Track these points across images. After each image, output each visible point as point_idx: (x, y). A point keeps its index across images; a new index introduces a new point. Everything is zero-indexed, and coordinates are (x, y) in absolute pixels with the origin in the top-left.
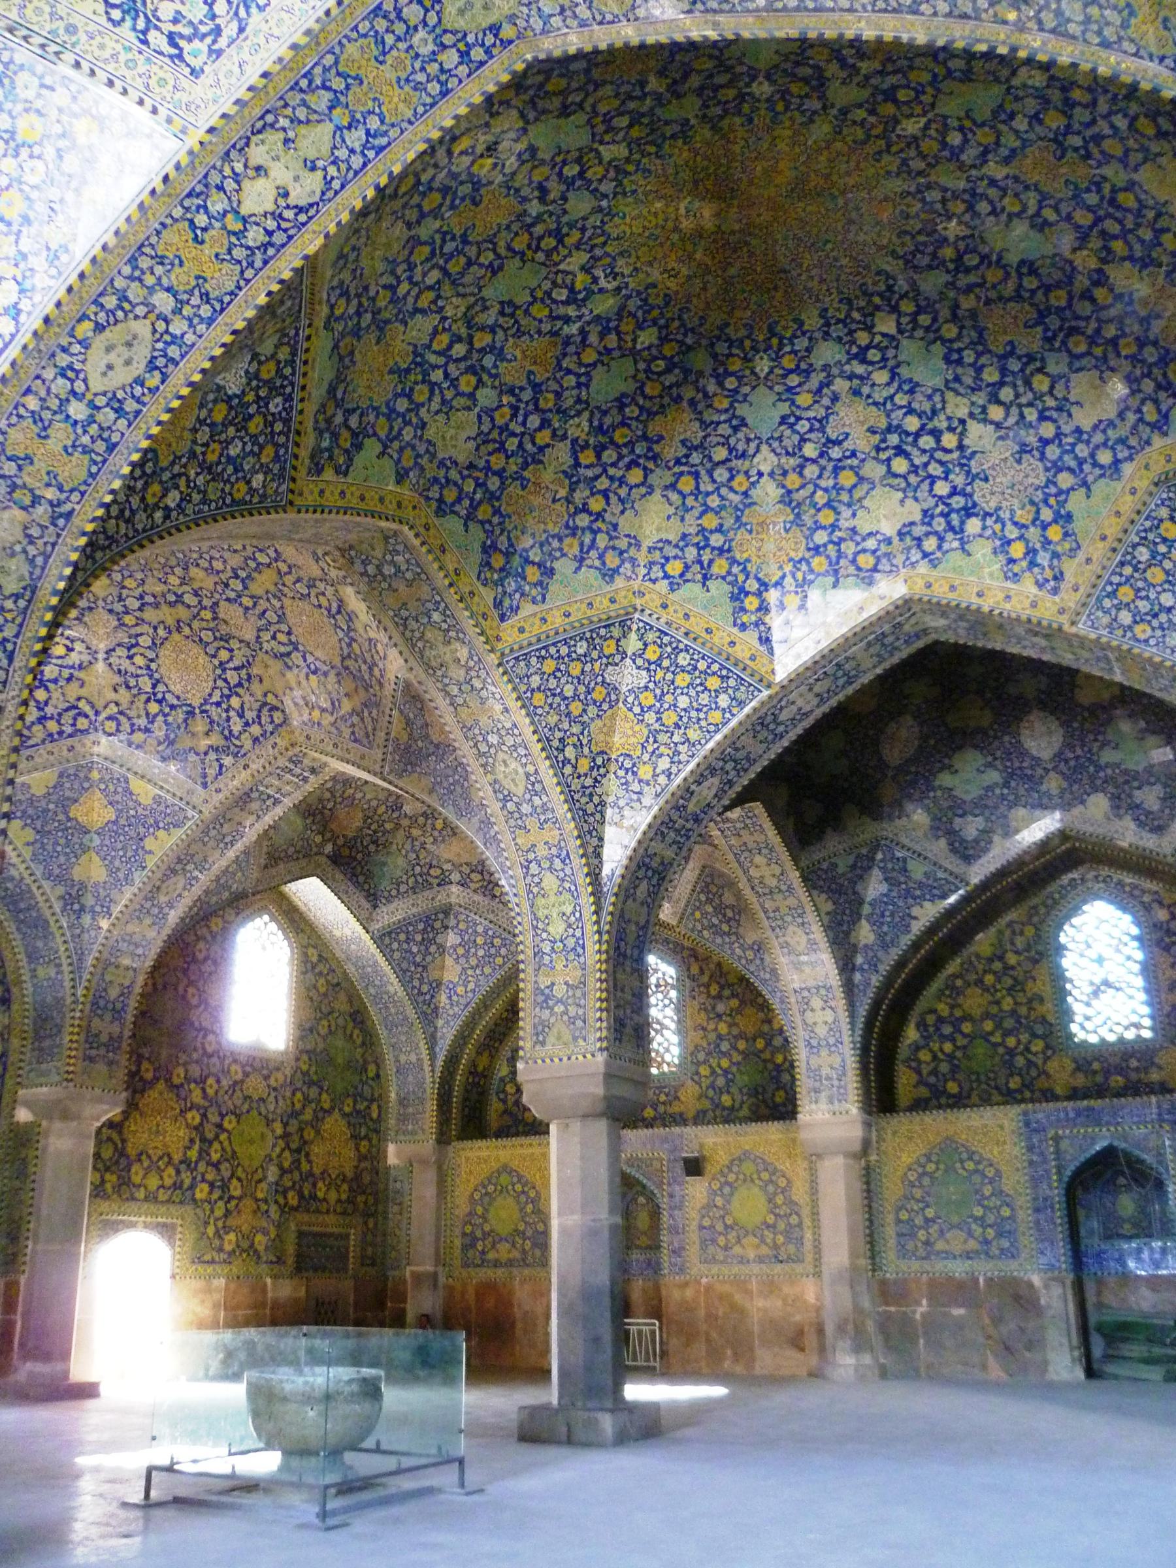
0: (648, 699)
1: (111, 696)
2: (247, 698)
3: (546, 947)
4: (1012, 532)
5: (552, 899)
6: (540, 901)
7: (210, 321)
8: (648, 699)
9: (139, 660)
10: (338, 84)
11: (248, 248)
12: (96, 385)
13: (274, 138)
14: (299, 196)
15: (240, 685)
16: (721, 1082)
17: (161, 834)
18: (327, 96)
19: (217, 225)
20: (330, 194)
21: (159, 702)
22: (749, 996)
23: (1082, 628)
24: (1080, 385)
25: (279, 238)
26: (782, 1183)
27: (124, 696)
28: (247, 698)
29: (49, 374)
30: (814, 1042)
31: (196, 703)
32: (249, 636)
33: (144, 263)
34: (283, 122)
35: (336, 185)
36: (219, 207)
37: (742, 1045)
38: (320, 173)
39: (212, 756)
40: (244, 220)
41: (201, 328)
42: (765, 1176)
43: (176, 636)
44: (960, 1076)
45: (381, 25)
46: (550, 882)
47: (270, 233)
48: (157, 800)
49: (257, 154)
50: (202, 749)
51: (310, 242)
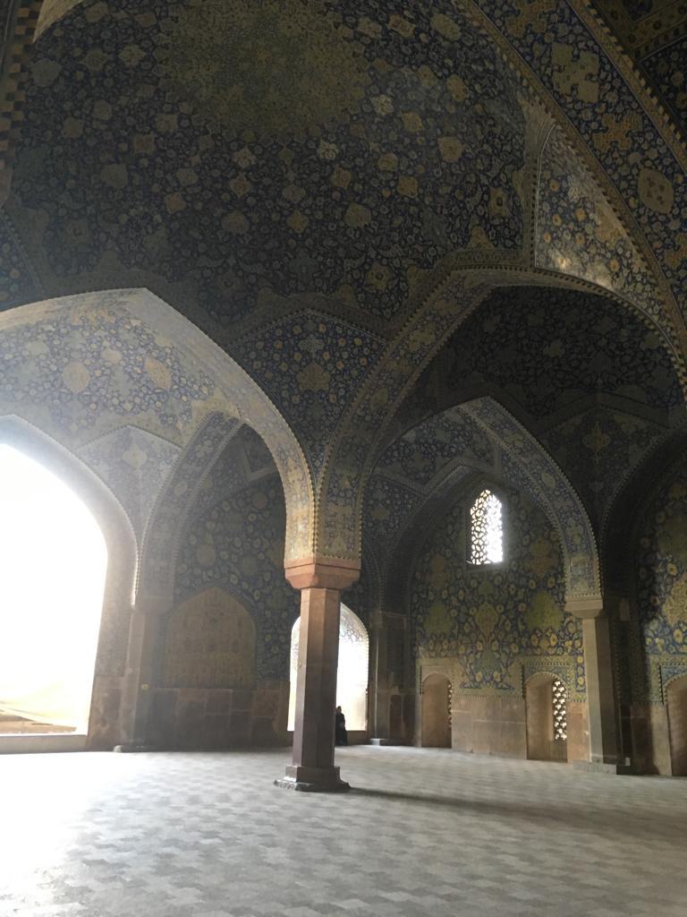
7: (657, 135)
10: (530, 39)
11: (618, 103)
12: (666, 209)
13: (557, 77)
14: (592, 68)
18: (536, 45)
19: (599, 118)
20: (596, 48)
25: (617, 83)
29: (648, 230)
33: (609, 161)
34: (548, 72)
35: (591, 43)
36: (590, 114)
38: (582, 53)
40: (601, 101)
41: (659, 141)
45: (498, 13)
47: (613, 88)
49: (564, 88)
51: (625, 64)
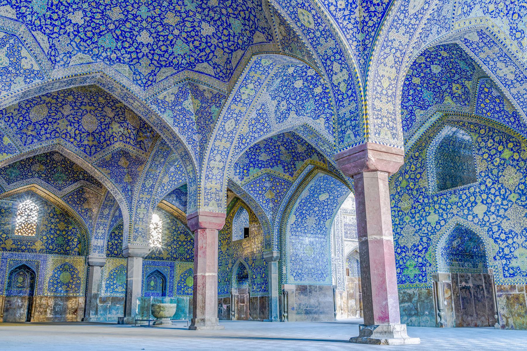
0: (172, 174)
1: (12, 111)
2: (50, 127)
3: (138, 219)
4: (238, 168)
5: (142, 209)
6: (139, 209)
8: (172, 174)
9: (28, 106)
15: (51, 123)
16: (50, 242)
17: (5, 154)
21: (24, 117)
22: (62, 219)
23: (243, 188)
24: (263, 154)
26: (76, 272)
27: (16, 112)
28: (50, 127)
30: (97, 237)
31: (33, 121)
32: (65, 114)
37: (58, 232)
39: (31, 137)
42: (71, 270)
43: (44, 105)
44: (118, 250)
46: (143, 206)
48: (9, 145)
50: (28, 135)
